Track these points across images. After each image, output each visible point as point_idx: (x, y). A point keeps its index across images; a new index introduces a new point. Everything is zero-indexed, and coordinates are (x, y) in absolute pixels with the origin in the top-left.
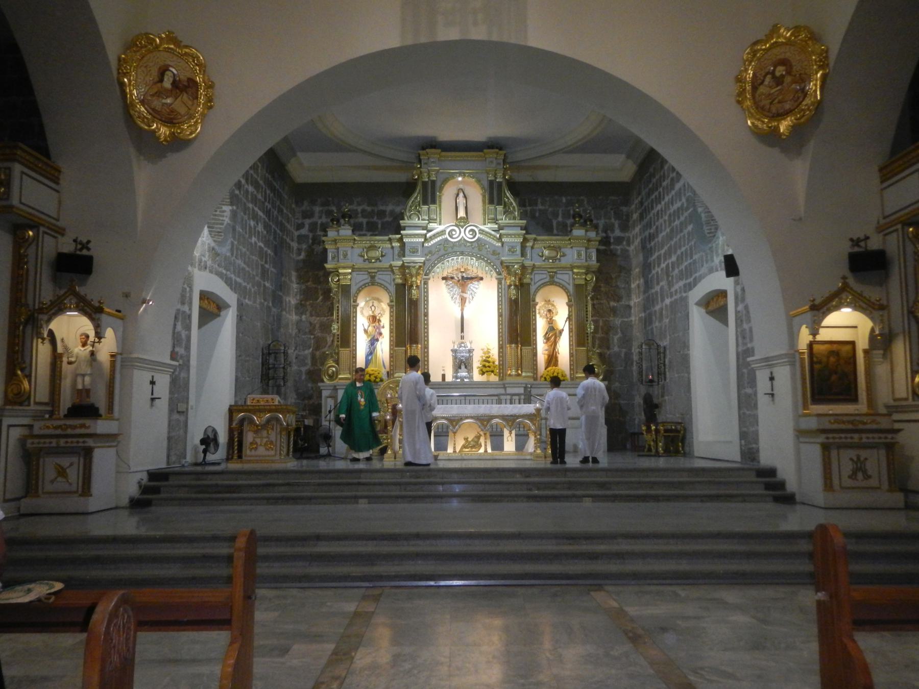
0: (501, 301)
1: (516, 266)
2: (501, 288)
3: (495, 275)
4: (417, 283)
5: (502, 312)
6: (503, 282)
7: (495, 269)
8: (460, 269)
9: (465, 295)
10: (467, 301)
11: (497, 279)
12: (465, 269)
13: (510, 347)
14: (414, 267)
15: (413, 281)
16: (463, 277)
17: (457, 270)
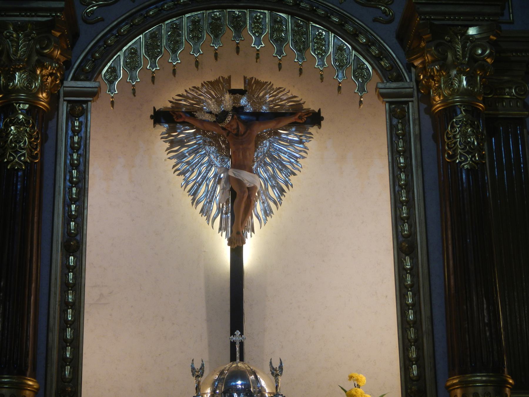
0: (408, 187)
1: (472, 31)
2: (405, 136)
3: (375, 80)
4: (33, 98)
5: (412, 234)
6: (412, 109)
7: (376, 60)
8: (228, 80)
9: (246, 177)
10: (259, 207)
11: (383, 95)
12: (248, 82)
13: (464, 385)
14: (18, 28)
15: (16, 90)
16: (238, 110)
17: (213, 84)
